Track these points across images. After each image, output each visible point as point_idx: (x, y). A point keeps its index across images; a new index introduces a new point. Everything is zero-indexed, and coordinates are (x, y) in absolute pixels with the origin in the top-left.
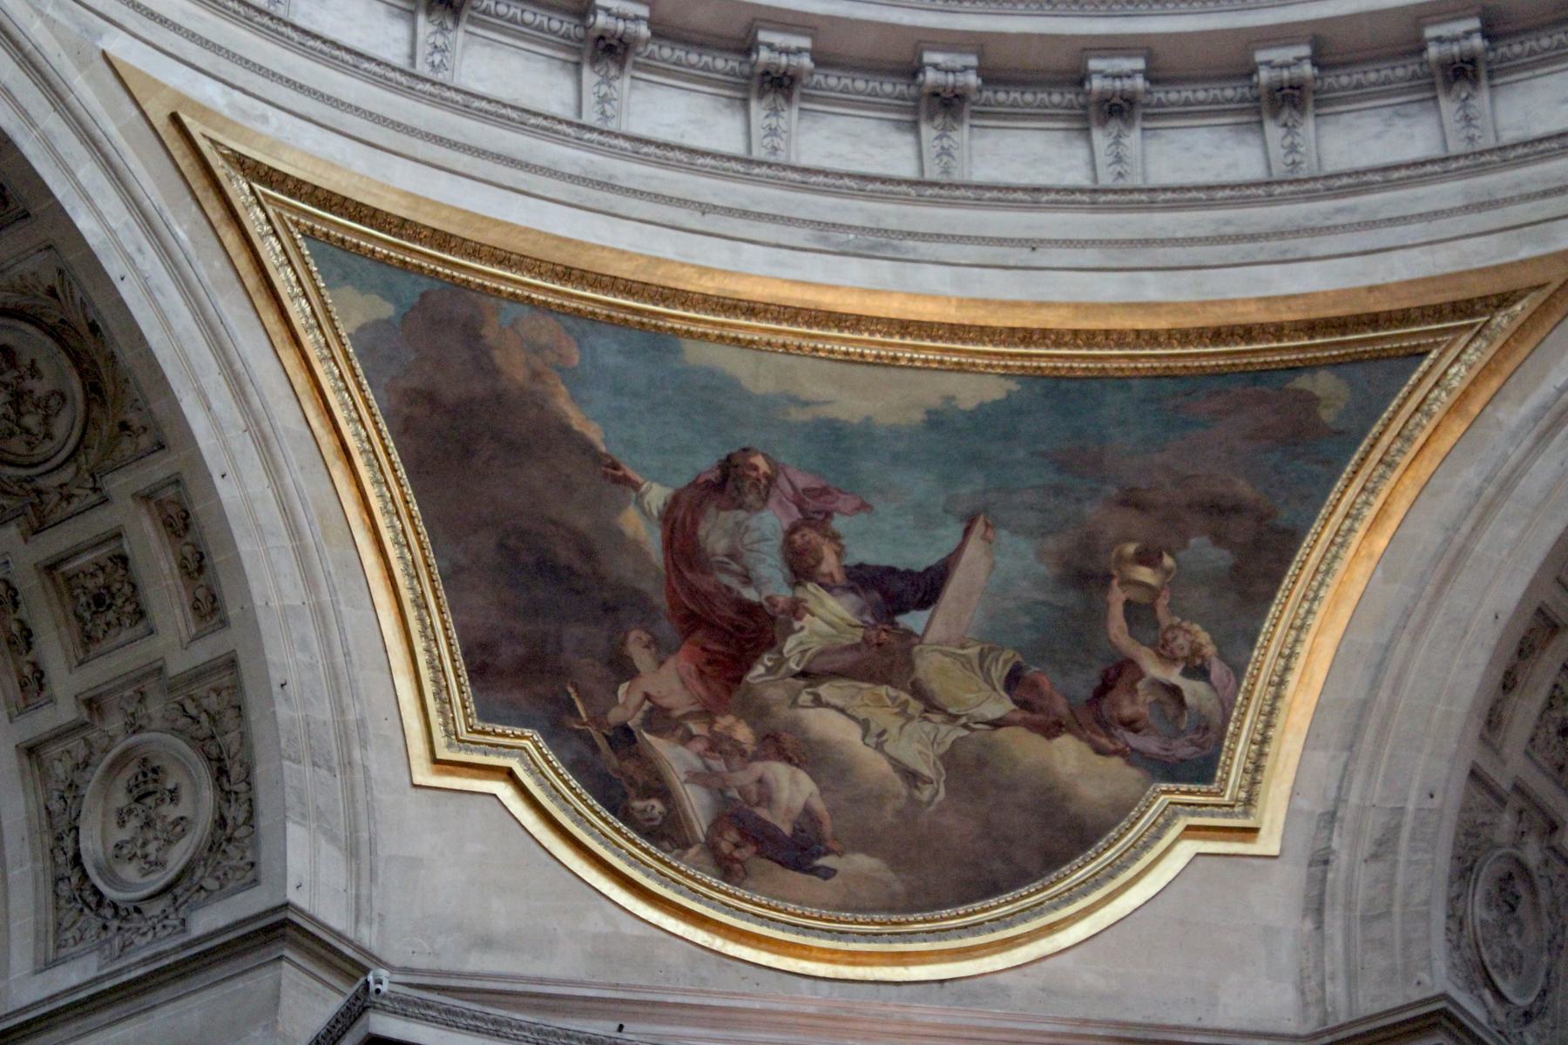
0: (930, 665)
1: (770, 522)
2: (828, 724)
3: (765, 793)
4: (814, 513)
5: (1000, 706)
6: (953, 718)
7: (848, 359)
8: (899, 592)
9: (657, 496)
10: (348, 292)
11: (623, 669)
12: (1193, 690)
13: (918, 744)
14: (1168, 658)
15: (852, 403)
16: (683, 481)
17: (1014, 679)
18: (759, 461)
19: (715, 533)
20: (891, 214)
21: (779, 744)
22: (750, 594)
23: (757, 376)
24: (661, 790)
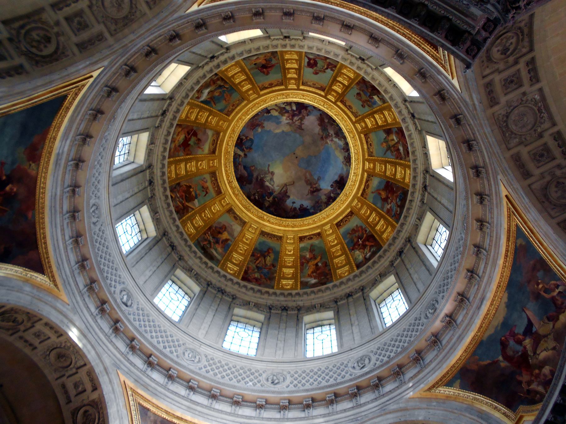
0: (542, 331)
1: (512, 343)
2: (543, 355)
3: (545, 375)
4: (513, 335)
5: (551, 324)
6: (550, 334)
7: (494, 316)
8: (529, 330)
9: (501, 358)
10: (454, 385)
11: (520, 383)
12: (560, 289)
13: (551, 344)
14: (554, 291)
15: (500, 318)
16: (500, 353)
17: (549, 320)
18: (503, 338)
19: (510, 353)
20: (479, 296)
21: (541, 365)
22: (520, 353)
23: (491, 331)
24: (537, 392)
